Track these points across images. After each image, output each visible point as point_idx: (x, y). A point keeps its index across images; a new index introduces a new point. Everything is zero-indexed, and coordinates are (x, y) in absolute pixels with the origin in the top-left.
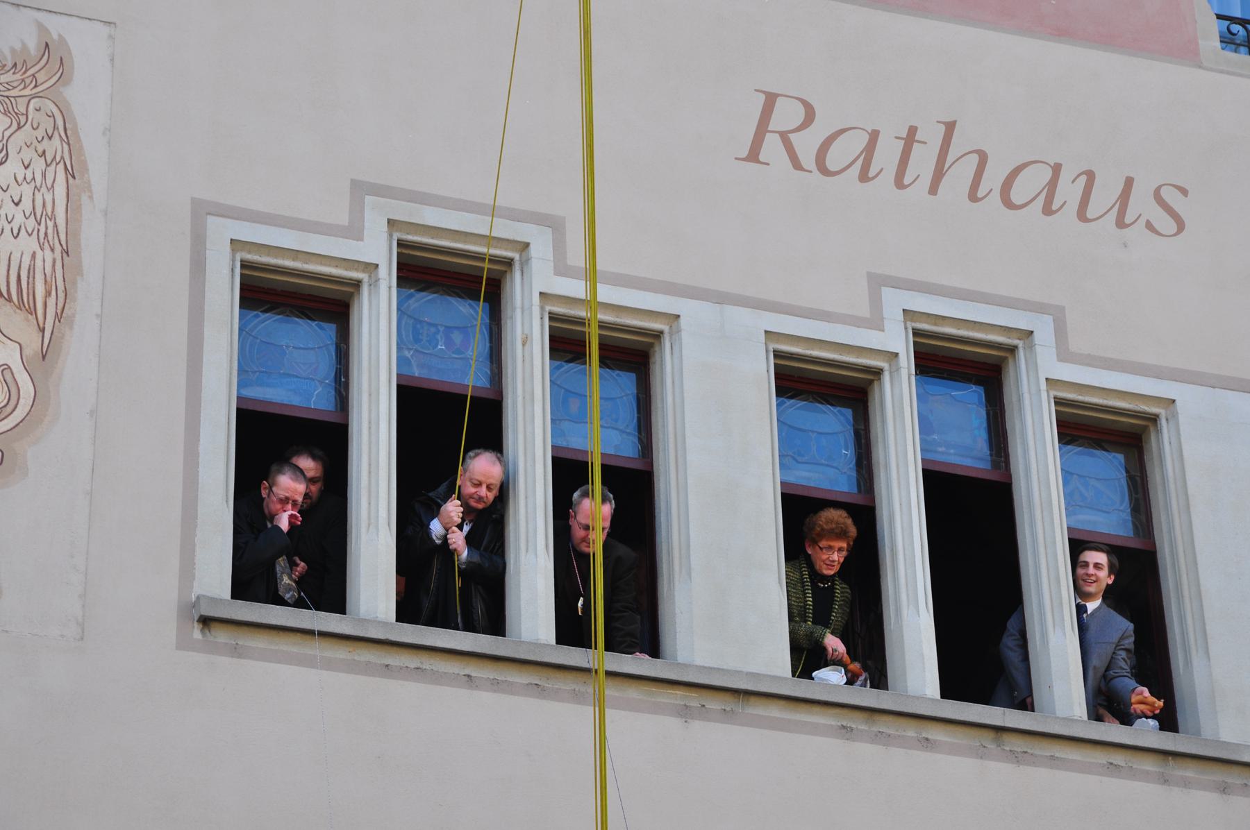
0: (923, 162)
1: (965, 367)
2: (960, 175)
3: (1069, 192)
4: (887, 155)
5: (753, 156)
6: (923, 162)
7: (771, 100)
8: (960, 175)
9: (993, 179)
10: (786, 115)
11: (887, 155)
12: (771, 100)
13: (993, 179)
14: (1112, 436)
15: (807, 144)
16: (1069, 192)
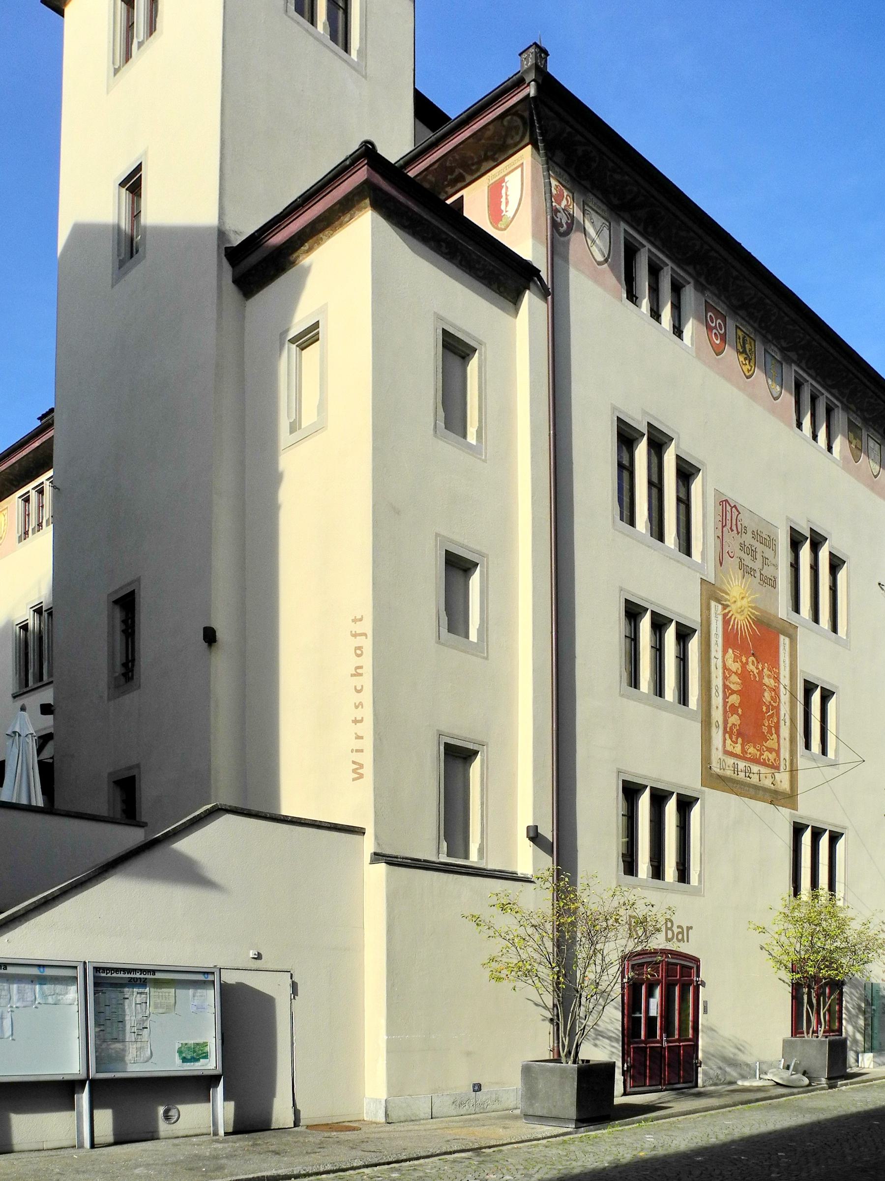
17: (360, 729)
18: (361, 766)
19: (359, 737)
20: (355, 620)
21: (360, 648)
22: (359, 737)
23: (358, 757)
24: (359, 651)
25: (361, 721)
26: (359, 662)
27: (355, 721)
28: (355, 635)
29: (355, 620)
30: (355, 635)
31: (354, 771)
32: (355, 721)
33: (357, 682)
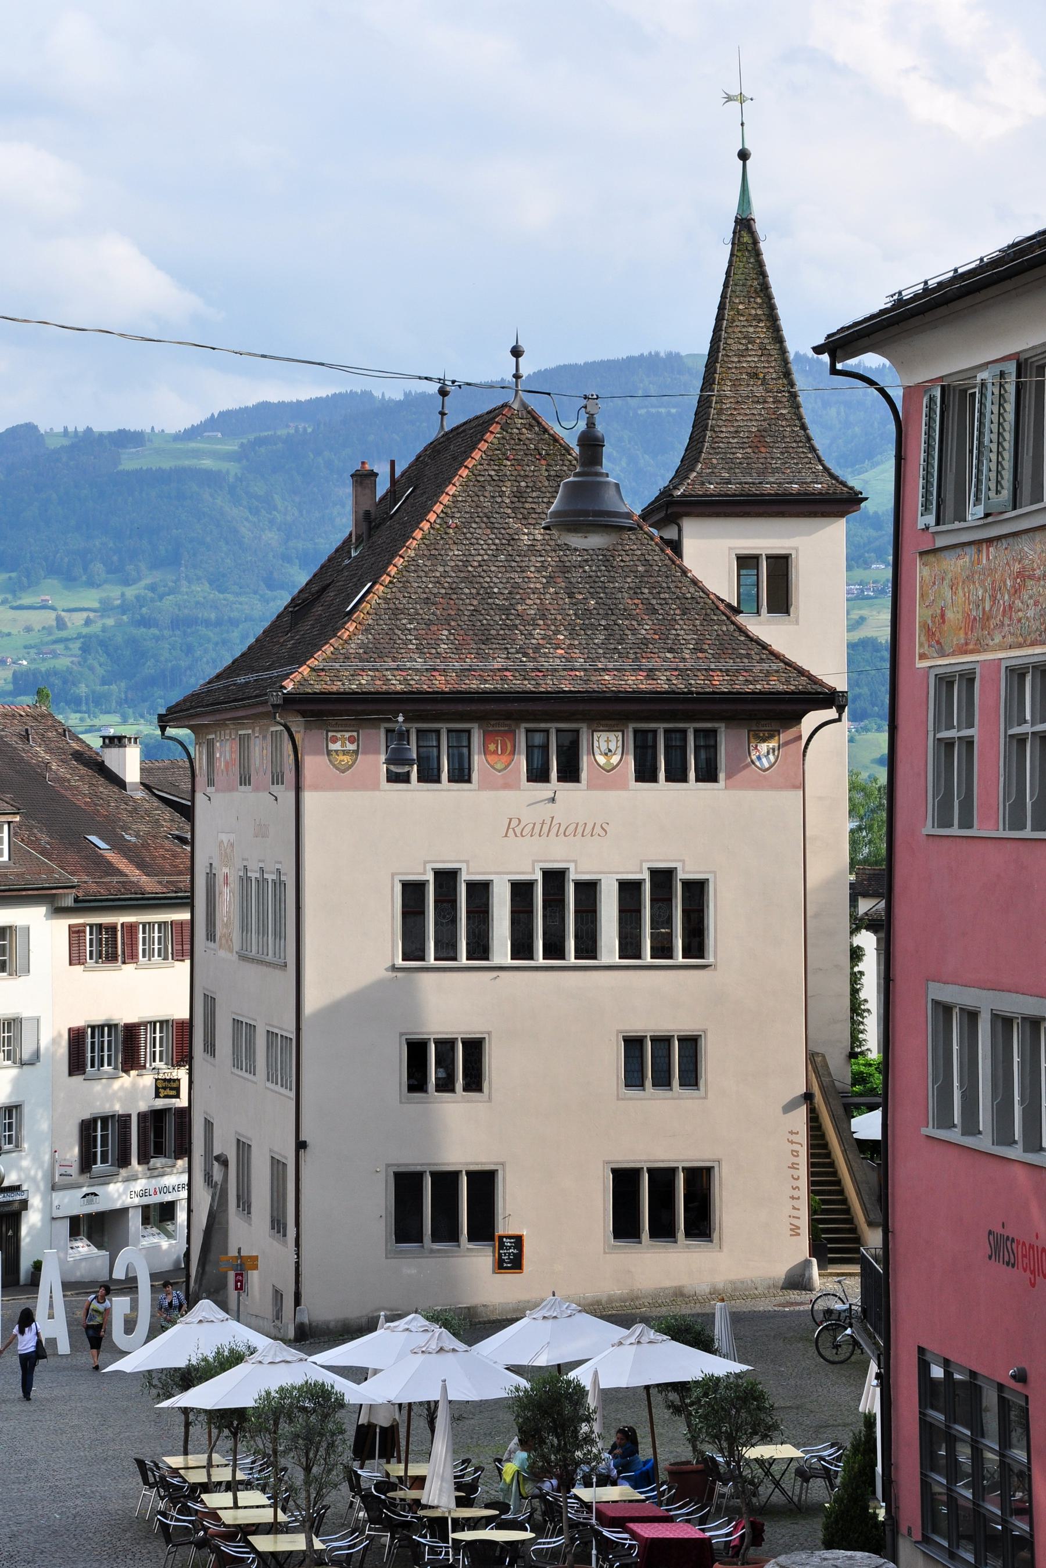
0: (546, 828)
1: (555, 878)
2: (554, 830)
3: (580, 830)
4: (537, 830)
5: (506, 836)
6: (546, 828)
7: (511, 819)
8: (554, 830)
9: (562, 830)
10: (514, 823)
11: (537, 830)
12: (511, 819)
13: (562, 830)
14: (588, 890)
15: (518, 830)
16: (580, 830)
17: (795, 1203)
18: (799, 1228)
19: (794, 1208)
20: (791, 1133)
21: (797, 1152)
22: (794, 1208)
23: (796, 1222)
24: (795, 1154)
25: (798, 1198)
26: (796, 1160)
27: (793, 1198)
28: (792, 1142)
29: (791, 1133)
30: (792, 1142)
31: (791, 1230)
32: (793, 1198)
33: (796, 1173)
